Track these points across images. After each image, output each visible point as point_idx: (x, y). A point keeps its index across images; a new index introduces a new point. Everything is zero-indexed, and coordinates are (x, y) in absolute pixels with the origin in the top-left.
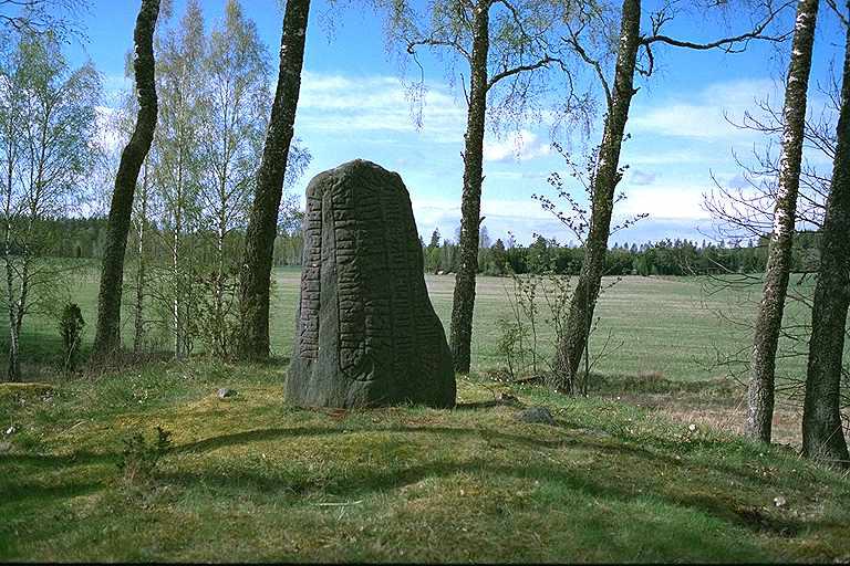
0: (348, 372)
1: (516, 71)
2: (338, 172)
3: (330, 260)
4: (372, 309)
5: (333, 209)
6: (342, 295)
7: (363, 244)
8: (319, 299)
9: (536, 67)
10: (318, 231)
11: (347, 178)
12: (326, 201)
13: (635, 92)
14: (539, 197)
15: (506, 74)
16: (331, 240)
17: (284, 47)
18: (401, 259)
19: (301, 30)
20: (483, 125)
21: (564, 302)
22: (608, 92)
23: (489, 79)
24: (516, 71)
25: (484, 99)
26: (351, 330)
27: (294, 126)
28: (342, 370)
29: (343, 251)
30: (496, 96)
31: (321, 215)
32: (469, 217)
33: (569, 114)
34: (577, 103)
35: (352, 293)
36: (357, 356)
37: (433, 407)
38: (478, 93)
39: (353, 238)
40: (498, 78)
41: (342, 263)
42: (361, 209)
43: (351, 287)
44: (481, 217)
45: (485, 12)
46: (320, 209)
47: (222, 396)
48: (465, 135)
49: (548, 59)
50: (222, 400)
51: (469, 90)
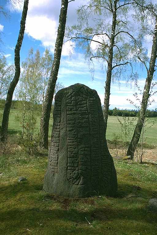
1: (119, 65)
6: (69, 145)
9: (124, 64)
13: (155, 71)
15: (117, 66)
17: (55, 52)
19: (61, 47)
22: (147, 70)
23: (112, 67)
24: (119, 65)
29: (70, 126)
30: (114, 71)
32: (106, 105)
33: (131, 78)
36: (75, 174)
37: (107, 196)
45: (112, 48)
49: (127, 63)
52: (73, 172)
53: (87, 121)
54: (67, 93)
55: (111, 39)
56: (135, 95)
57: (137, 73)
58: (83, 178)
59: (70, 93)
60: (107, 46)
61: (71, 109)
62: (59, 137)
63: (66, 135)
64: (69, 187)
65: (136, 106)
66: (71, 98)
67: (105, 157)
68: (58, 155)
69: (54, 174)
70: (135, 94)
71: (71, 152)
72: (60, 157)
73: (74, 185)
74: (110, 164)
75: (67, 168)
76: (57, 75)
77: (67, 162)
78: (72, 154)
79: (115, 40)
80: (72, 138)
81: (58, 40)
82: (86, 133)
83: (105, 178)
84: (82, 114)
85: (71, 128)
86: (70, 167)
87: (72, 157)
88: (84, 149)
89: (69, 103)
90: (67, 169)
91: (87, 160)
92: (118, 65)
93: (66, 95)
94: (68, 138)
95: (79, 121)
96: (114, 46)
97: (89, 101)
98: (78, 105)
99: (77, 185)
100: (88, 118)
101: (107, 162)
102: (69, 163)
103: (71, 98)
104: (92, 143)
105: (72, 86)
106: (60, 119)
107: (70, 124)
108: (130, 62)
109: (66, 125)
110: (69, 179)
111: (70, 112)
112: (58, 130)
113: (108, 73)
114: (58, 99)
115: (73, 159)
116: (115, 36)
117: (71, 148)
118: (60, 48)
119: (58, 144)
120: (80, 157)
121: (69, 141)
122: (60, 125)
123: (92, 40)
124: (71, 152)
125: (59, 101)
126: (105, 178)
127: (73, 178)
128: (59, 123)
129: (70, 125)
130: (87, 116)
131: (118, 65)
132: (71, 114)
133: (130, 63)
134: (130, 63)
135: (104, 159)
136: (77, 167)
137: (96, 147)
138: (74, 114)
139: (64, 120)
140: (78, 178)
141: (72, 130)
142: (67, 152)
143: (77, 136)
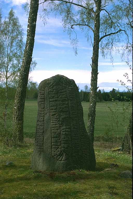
1: (109, 35)
3: (48, 114)
6: (52, 127)
9: (116, 33)
10: (43, 103)
14: (120, 81)
15: (106, 36)
17: (28, 28)
18: (75, 113)
19: (35, 22)
20: (98, 54)
24: (109, 35)
25: (99, 45)
29: (53, 111)
31: (44, 96)
33: (127, 49)
38: (96, 43)
40: (103, 37)
44: (97, 87)
45: (99, 14)
48: (92, 58)
49: (120, 30)
51: (93, 43)
52: (57, 150)
53: (67, 106)
54: (48, 83)
58: (65, 155)
59: (51, 84)
61: (53, 97)
62: (43, 121)
66: (53, 87)
67: (84, 136)
70: (125, 74)
71: (54, 133)
75: (52, 147)
78: (55, 134)
80: (55, 121)
82: (67, 117)
84: (62, 101)
85: (54, 113)
86: (54, 145)
87: (56, 137)
89: (51, 92)
90: (51, 148)
92: (108, 35)
93: (49, 85)
94: (51, 122)
95: (60, 106)
96: (102, 10)
97: (68, 89)
98: (59, 93)
99: (60, 161)
100: (68, 104)
102: (54, 143)
103: (53, 87)
106: (44, 106)
107: (52, 109)
108: (123, 29)
109: (49, 110)
110: (53, 156)
112: (43, 115)
115: (56, 139)
118: (34, 24)
119: (43, 127)
120: (62, 137)
121: (53, 124)
124: (54, 133)
125: (43, 91)
126: (84, 155)
127: (57, 155)
128: (43, 109)
129: (53, 110)
130: (67, 102)
131: (108, 35)
132: (53, 101)
133: (124, 30)
134: (124, 30)
135: (83, 138)
136: (60, 145)
137: (75, 128)
138: (56, 100)
139: (48, 106)
140: (61, 155)
141: (55, 114)
143: (59, 119)
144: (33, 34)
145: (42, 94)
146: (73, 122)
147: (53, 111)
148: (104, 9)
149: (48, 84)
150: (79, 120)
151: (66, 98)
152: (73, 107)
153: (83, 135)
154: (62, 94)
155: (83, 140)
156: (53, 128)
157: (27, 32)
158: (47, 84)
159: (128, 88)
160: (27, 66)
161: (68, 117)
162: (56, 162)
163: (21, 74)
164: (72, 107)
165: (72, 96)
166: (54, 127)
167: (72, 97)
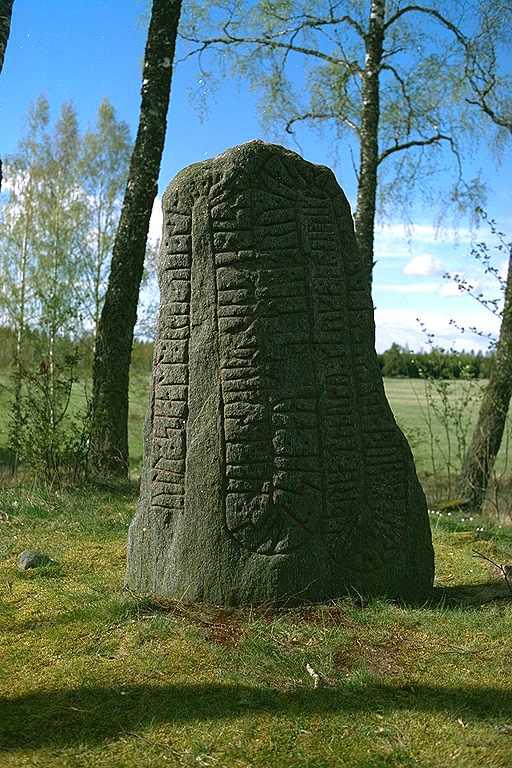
0: (237, 539)
1: (407, 146)
2: (221, 163)
3: (205, 326)
4: (284, 417)
5: (212, 230)
7: (267, 296)
8: (185, 399)
11: (237, 171)
12: (199, 215)
14: (453, 277)
15: (397, 148)
16: (208, 287)
18: (337, 325)
19: (167, 60)
20: (374, 203)
21: (465, 404)
23: (380, 153)
24: (407, 146)
26: (246, 459)
27: (158, 182)
28: (229, 534)
29: (232, 308)
31: (189, 242)
33: (456, 203)
34: (465, 190)
35: (247, 388)
36: (257, 507)
37: (398, 603)
38: (369, 166)
39: (248, 284)
40: (389, 152)
41: (227, 331)
42: (262, 230)
43: (246, 376)
45: (376, 76)
46: (188, 232)
47: (22, 566)
49: (440, 137)
50: (22, 576)
51: (358, 164)
52: (248, 499)
55: (369, 36)
56: (479, 252)
57: (482, 182)
60: (354, 68)
62: (186, 359)
63: (215, 350)
64: (235, 563)
65: (481, 299)
67: (378, 436)
68: (183, 435)
69: (170, 514)
70: (477, 249)
72: (192, 442)
73: (254, 555)
74: (401, 465)
76: (156, 179)
77: (225, 458)
78: (241, 423)
79: (386, 45)
80: (240, 361)
81: (156, 30)
83: (380, 524)
85: (237, 319)
88: (293, 405)
90: (223, 492)
91: (306, 447)
93: (211, 185)
94: (223, 362)
96: (384, 67)
101: (386, 459)
104: (323, 378)
105: (236, 153)
106: (189, 285)
107: (229, 303)
108: (449, 135)
109: (213, 307)
110: (234, 531)
111: (229, 255)
112: (181, 331)
113: (363, 178)
114: (176, 204)
116: (386, 26)
117: (237, 399)
119: (183, 387)
122: (187, 313)
123: (291, 47)
126: (380, 524)
133: (450, 139)
134: (450, 139)
135: (374, 444)
137: (338, 397)
139: (206, 289)
142: (223, 419)
144: (161, 102)
145: (177, 233)
146: (330, 364)
147: (232, 308)
148: (388, 68)
149: (210, 180)
150: (358, 355)
151: (295, 251)
152: (330, 293)
153: (375, 431)
154: (274, 230)
155: (374, 452)
156: (233, 395)
157: (142, 93)
158: (204, 184)
159: (481, 299)
160: (143, 212)
161: (303, 342)
162: (244, 560)
163: (121, 242)
164: (324, 294)
165: (321, 243)
166: (237, 390)
167: (323, 247)
